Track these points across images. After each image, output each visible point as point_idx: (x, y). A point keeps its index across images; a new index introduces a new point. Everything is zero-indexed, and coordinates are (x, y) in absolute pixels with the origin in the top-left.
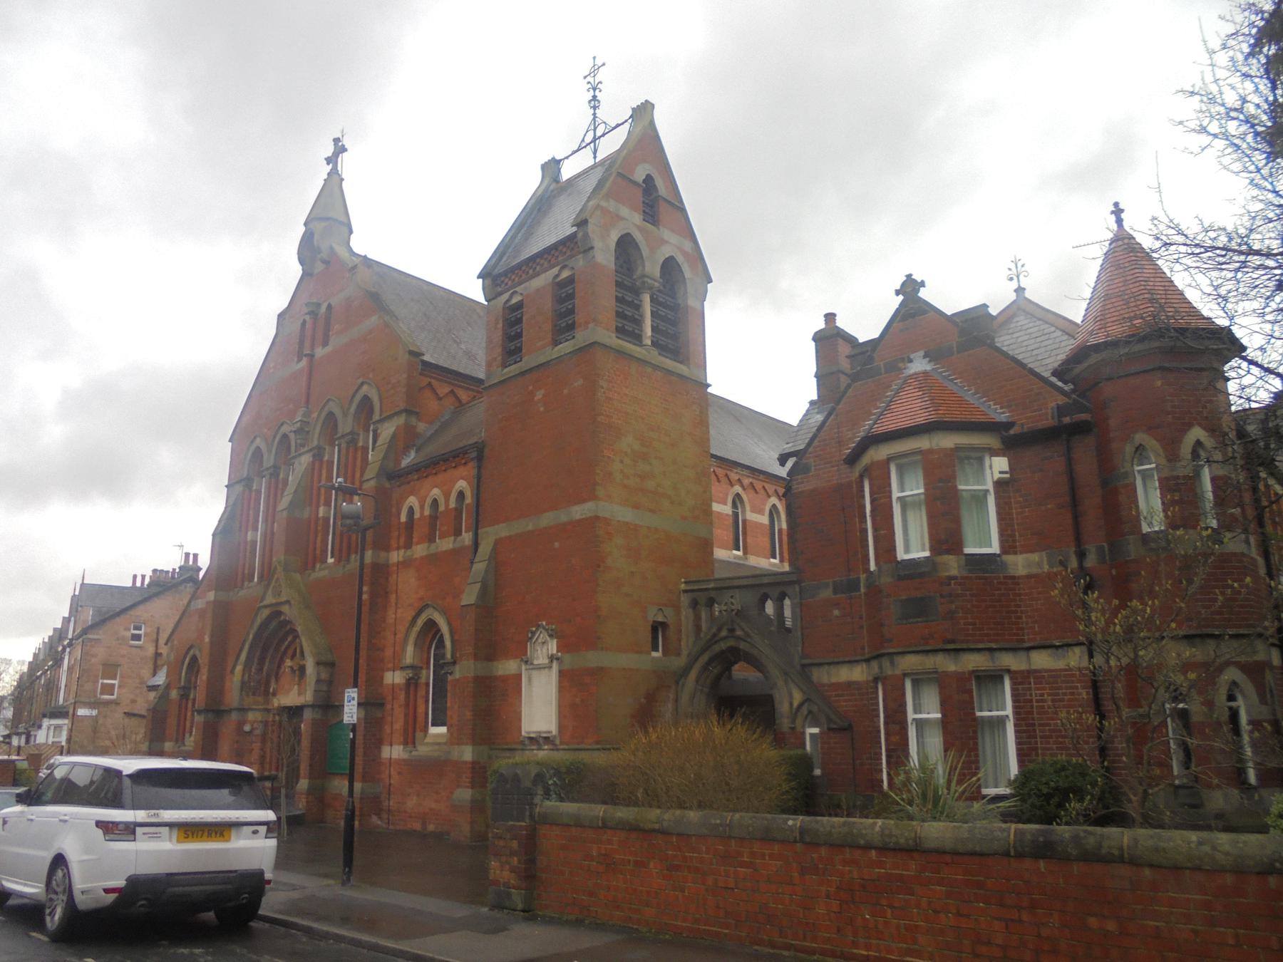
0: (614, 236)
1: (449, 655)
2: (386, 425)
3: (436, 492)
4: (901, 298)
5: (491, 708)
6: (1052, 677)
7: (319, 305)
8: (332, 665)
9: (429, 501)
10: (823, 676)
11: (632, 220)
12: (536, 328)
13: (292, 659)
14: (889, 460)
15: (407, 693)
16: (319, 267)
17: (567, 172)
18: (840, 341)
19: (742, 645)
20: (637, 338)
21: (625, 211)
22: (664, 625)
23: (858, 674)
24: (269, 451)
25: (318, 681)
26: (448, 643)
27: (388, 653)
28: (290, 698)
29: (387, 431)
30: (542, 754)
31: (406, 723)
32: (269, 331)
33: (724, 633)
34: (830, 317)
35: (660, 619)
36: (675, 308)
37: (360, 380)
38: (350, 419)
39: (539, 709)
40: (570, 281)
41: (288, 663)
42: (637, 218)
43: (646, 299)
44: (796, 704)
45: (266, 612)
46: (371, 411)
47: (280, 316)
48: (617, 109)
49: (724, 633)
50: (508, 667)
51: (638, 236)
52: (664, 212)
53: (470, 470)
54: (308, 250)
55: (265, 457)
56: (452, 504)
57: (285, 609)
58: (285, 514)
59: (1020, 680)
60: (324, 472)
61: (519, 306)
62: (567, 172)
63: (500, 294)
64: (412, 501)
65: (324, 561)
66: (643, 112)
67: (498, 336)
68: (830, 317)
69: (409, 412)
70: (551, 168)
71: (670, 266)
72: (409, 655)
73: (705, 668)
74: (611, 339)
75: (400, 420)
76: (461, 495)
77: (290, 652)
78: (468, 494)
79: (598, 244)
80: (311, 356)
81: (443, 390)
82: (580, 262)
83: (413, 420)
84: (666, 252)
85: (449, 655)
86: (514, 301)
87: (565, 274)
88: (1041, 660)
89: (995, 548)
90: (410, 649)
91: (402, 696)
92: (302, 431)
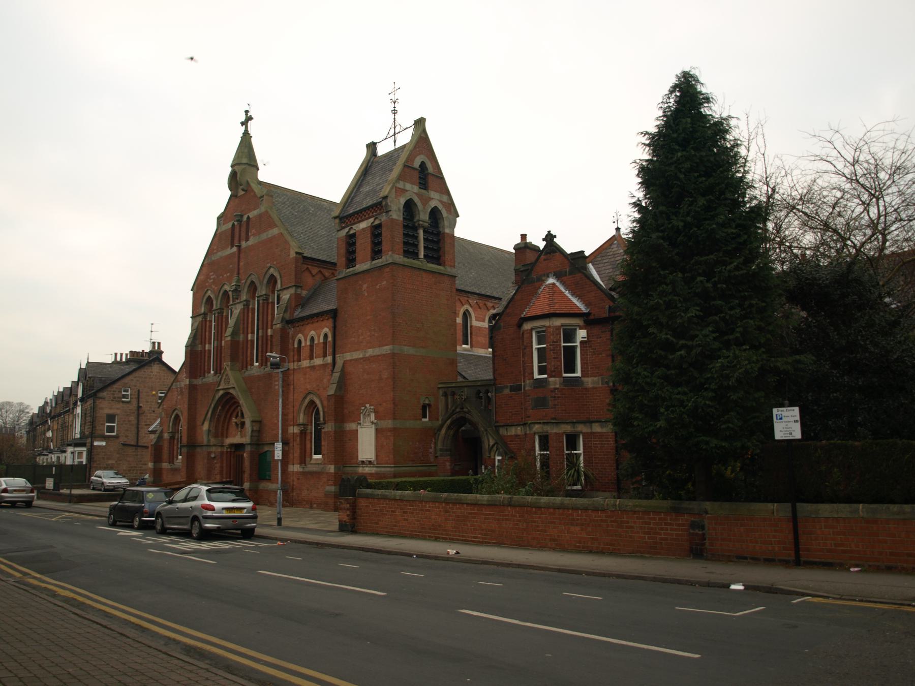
0: (402, 201)
1: (322, 419)
2: (285, 292)
3: (313, 333)
4: (541, 245)
5: (344, 446)
6: (601, 435)
7: (242, 216)
8: (260, 422)
9: (309, 338)
10: (503, 431)
11: (412, 189)
12: (364, 246)
13: (237, 417)
14: (532, 329)
15: (301, 440)
16: (241, 193)
17: (382, 150)
18: (528, 250)
19: (467, 416)
20: (415, 255)
21: (408, 186)
22: (429, 405)
23: (519, 430)
24: (217, 299)
25: (252, 431)
26: (321, 413)
27: (290, 416)
28: (236, 439)
29: (286, 296)
30: (367, 470)
31: (301, 453)
32: (212, 227)
33: (458, 410)
34: (524, 236)
35: (427, 402)
36: (439, 234)
37: (269, 265)
38: (264, 288)
39: (366, 445)
40: (379, 226)
41: (234, 420)
42: (416, 189)
43: (421, 232)
44: (491, 444)
45: (221, 393)
46: (276, 282)
47: (218, 218)
48: (407, 120)
49: (458, 410)
50: (352, 426)
51: (416, 199)
52: (430, 179)
53: (330, 323)
54: (234, 181)
55: (214, 302)
56: (322, 340)
57: (231, 391)
58: (229, 338)
59: (587, 436)
60: (250, 314)
61: (354, 235)
62: (382, 150)
63: (344, 228)
64: (300, 336)
65: (252, 364)
66: (420, 123)
67: (343, 251)
68: (524, 236)
69: (297, 287)
70: (372, 147)
71: (435, 214)
72: (301, 419)
73: (449, 428)
74: (400, 258)
75: (292, 291)
76: (326, 336)
77: (235, 414)
78: (330, 339)
79: (394, 207)
80: (239, 247)
81: (315, 271)
82: (384, 218)
83: (299, 291)
84: (433, 204)
85: (322, 419)
86: (351, 232)
87: (377, 222)
88: (597, 428)
89: (578, 374)
90: (302, 415)
91: (298, 439)
92: (237, 291)
